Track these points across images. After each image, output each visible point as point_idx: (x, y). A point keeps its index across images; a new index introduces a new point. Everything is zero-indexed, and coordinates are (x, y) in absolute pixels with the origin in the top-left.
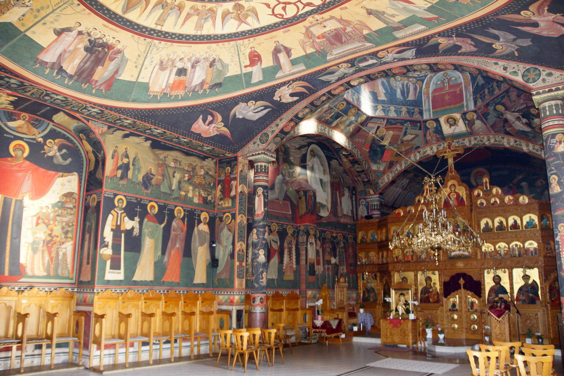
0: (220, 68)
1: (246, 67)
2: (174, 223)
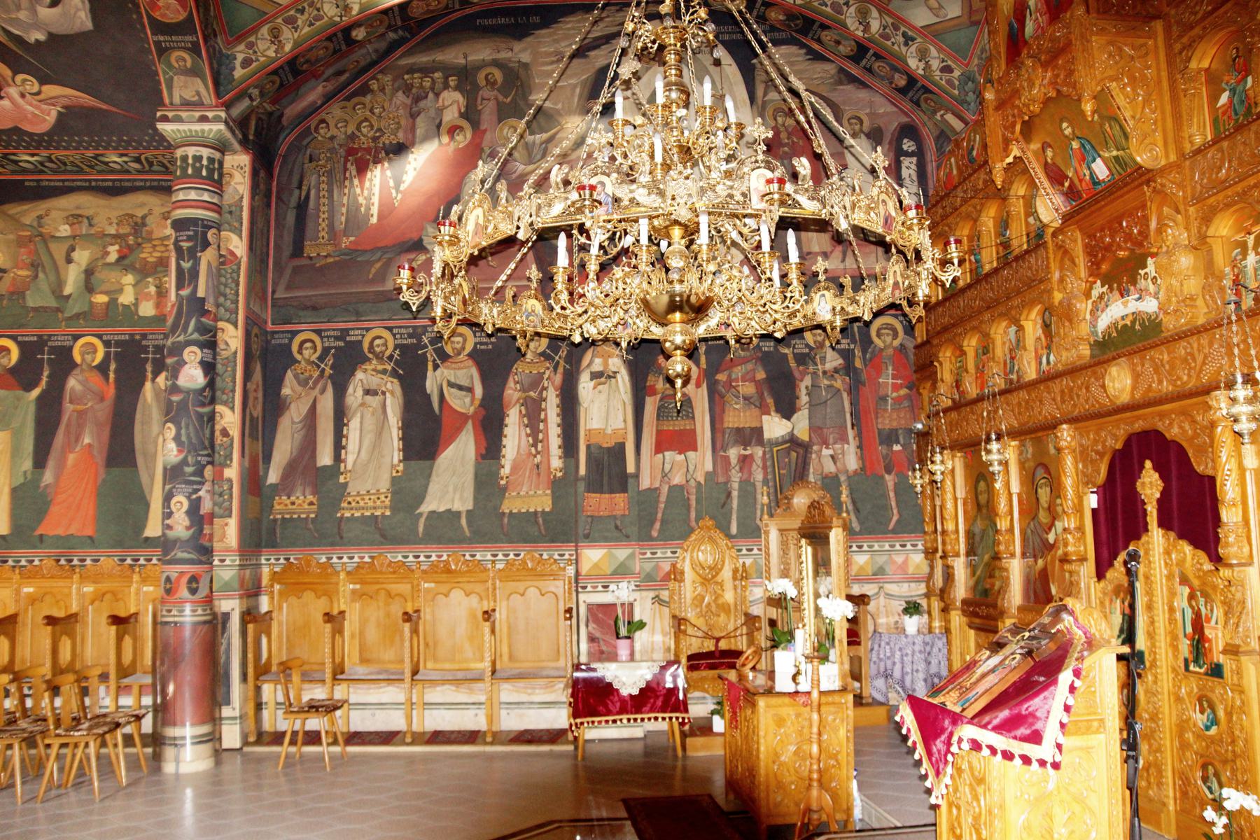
2: (72, 383)
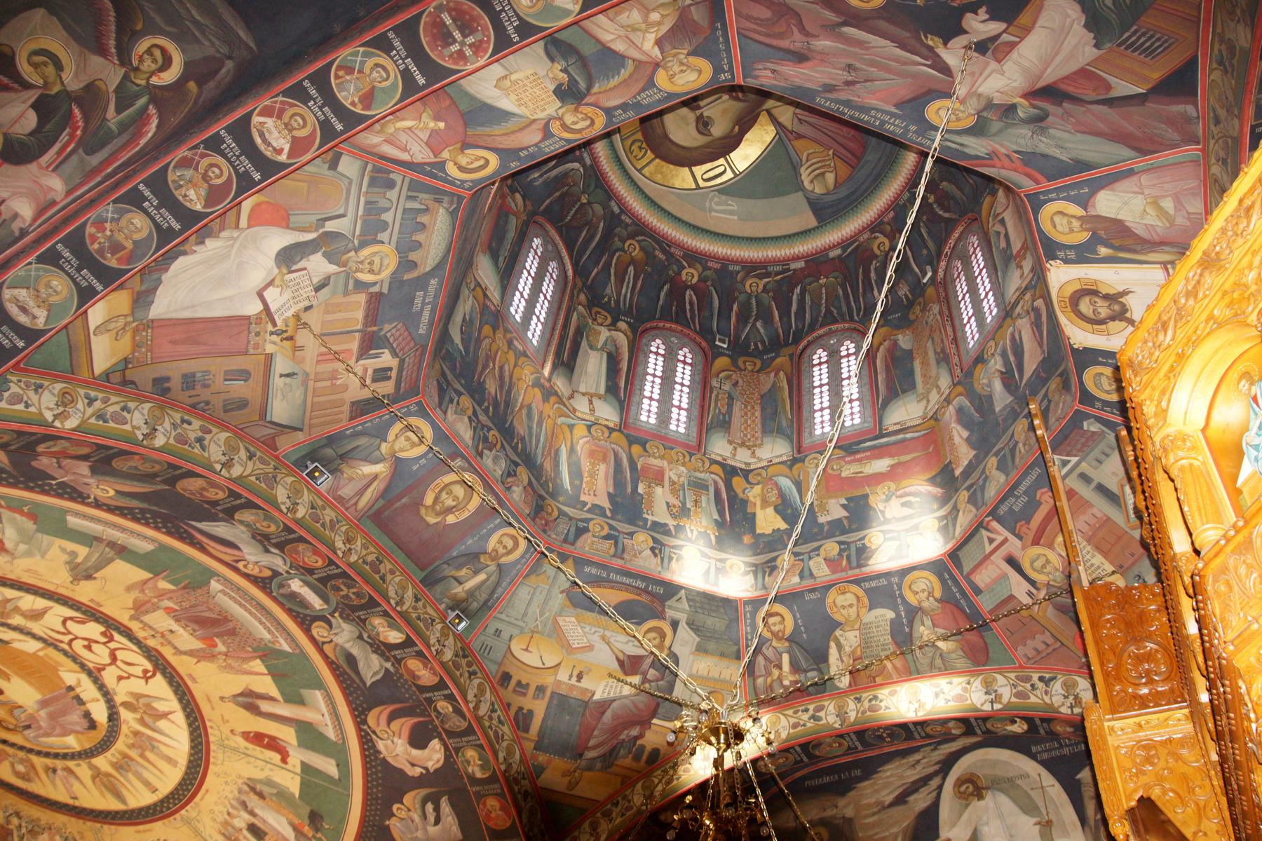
0: (275, 791)
1: (284, 760)
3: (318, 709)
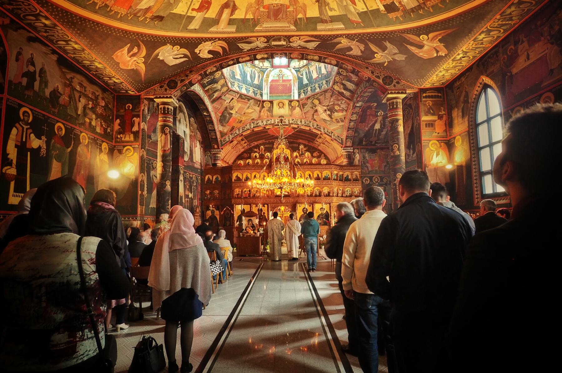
1: (193, 10)
3: (225, 28)
